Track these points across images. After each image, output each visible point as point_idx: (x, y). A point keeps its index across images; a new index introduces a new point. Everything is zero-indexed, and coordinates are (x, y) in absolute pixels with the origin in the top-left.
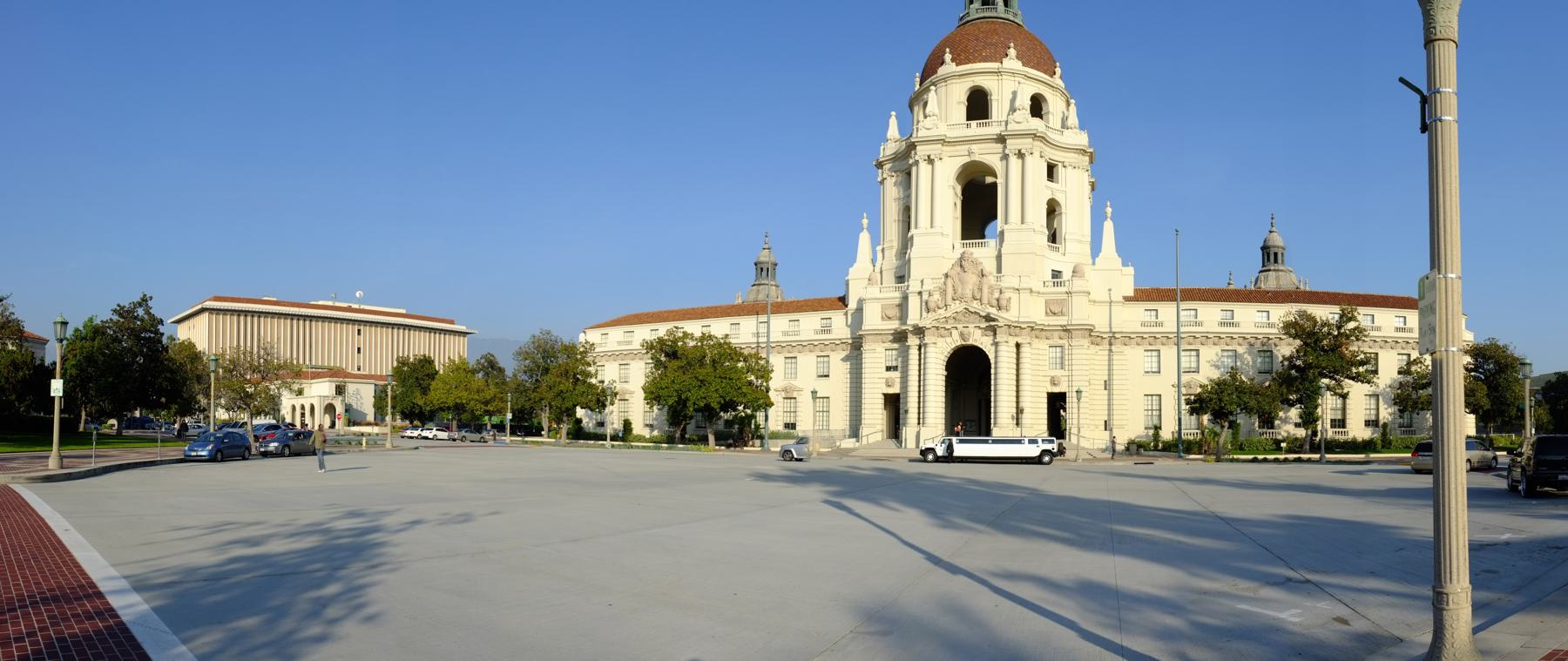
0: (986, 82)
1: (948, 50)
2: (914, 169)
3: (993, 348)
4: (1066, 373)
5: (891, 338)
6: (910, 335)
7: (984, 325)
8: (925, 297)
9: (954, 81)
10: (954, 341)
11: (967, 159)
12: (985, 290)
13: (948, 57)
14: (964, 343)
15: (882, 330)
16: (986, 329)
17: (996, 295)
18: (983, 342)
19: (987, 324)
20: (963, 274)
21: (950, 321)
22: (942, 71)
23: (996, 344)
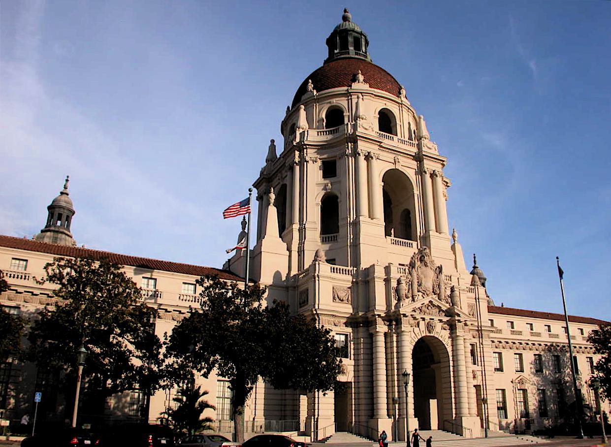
0: (394, 109)
1: (360, 72)
2: (351, 160)
3: (450, 341)
4: (479, 368)
5: (344, 320)
6: (379, 320)
7: (445, 319)
8: (394, 284)
9: (369, 98)
10: (422, 332)
11: (393, 167)
12: (443, 287)
13: (361, 77)
14: (429, 334)
15: (340, 312)
16: (447, 322)
17: (448, 292)
18: (443, 335)
19: (448, 318)
20: (424, 267)
21: (417, 311)
22: (355, 86)
23: (453, 337)
